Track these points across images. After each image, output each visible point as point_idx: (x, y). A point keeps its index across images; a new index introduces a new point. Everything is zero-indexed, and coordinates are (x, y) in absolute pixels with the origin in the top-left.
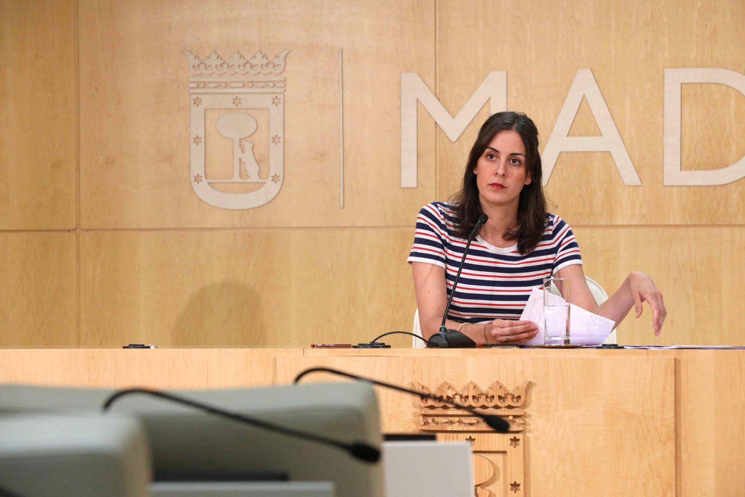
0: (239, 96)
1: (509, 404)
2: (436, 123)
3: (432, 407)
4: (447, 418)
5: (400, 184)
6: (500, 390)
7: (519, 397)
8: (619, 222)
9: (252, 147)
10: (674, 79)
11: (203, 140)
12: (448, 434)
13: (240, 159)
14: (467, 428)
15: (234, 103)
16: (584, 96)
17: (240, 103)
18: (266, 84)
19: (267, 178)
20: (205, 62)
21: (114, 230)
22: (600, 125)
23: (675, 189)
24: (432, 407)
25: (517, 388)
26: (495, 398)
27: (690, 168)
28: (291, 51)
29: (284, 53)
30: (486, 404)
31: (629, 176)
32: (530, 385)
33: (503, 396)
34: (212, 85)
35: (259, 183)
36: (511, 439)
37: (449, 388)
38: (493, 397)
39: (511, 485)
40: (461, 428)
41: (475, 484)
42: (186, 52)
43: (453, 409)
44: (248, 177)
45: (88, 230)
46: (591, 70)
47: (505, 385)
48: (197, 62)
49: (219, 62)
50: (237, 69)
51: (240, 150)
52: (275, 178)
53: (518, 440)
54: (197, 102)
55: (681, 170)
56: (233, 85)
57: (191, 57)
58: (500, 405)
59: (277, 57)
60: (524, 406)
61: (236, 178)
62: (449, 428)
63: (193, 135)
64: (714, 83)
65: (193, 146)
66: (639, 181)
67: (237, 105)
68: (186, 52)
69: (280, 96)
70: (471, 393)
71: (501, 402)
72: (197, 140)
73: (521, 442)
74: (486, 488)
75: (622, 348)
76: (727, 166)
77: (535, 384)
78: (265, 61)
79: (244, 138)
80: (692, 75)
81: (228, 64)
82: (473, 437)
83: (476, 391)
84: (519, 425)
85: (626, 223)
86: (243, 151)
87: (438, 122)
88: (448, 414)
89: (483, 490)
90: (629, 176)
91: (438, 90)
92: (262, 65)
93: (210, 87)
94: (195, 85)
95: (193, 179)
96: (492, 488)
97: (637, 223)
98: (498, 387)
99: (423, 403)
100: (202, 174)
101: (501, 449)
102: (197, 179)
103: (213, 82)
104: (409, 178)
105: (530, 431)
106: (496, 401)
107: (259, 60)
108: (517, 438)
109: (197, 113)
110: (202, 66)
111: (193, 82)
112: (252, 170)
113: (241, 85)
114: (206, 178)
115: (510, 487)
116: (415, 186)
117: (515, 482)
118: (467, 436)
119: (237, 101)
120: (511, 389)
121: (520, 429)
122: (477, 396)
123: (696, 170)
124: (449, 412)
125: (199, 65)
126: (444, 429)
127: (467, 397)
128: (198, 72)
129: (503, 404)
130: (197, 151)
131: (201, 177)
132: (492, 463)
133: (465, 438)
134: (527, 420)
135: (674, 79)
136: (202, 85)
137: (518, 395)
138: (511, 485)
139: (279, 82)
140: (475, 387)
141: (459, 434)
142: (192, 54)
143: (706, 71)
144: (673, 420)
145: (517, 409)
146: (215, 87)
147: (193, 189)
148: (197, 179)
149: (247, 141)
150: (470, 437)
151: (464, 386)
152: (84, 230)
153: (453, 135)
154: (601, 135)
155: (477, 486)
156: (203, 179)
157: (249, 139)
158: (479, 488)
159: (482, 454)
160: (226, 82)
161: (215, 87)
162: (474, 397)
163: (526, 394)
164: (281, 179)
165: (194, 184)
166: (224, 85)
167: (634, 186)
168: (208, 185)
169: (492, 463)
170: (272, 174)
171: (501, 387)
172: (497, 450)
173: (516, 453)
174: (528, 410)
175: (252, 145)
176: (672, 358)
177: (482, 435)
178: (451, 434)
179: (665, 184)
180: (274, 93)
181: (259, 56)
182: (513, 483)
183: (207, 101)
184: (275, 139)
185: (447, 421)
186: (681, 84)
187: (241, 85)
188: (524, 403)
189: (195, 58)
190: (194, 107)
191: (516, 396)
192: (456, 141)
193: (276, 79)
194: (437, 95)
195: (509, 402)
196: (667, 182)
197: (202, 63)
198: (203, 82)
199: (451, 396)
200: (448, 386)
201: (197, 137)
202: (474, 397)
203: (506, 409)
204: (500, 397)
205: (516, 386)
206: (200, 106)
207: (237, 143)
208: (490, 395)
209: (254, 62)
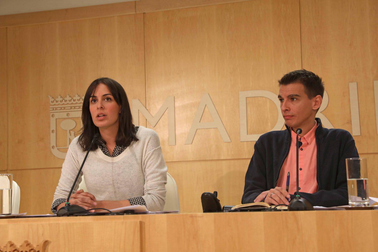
0: (69, 113)
2: (146, 120)
6: (27, 247)
8: (222, 158)
9: (74, 133)
10: (243, 95)
11: (55, 131)
13: (70, 139)
15: (67, 115)
16: (206, 105)
17: (70, 116)
23: (245, 143)
27: (251, 134)
32: (46, 243)
42: (49, 96)
45: (12, 170)
47: (32, 243)
48: (53, 100)
49: (61, 99)
50: (68, 102)
51: (70, 134)
55: (247, 134)
56: (66, 108)
57: (50, 98)
63: (51, 129)
64: (260, 97)
65: (52, 134)
66: (230, 140)
67: (68, 116)
68: (49, 96)
72: (53, 131)
77: (51, 242)
79: (71, 130)
80: (250, 94)
85: (225, 159)
86: (70, 135)
91: (147, 106)
92: (78, 100)
93: (58, 110)
94: (52, 109)
95: (51, 147)
98: (25, 244)
100: (55, 145)
102: (53, 147)
109: (53, 121)
113: (70, 108)
114: (57, 147)
119: (68, 115)
120: (35, 246)
123: (254, 134)
128: (53, 104)
130: (53, 136)
131: (54, 146)
142: (51, 96)
146: (60, 110)
147: (51, 152)
148: (53, 147)
149: (72, 131)
151: (5, 246)
156: (55, 147)
157: (73, 130)
160: (64, 107)
161: (60, 110)
165: (52, 149)
166: (63, 108)
167: (228, 142)
168: (57, 150)
171: (28, 244)
175: (74, 132)
176: (138, 221)
181: (77, 96)
183: (57, 115)
186: (246, 98)
187: (70, 108)
189: (52, 98)
190: (51, 118)
192: (155, 127)
194: (147, 108)
197: (55, 100)
198: (55, 108)
205: (38, 245)
206: (54, 117)
207: (68, 132)
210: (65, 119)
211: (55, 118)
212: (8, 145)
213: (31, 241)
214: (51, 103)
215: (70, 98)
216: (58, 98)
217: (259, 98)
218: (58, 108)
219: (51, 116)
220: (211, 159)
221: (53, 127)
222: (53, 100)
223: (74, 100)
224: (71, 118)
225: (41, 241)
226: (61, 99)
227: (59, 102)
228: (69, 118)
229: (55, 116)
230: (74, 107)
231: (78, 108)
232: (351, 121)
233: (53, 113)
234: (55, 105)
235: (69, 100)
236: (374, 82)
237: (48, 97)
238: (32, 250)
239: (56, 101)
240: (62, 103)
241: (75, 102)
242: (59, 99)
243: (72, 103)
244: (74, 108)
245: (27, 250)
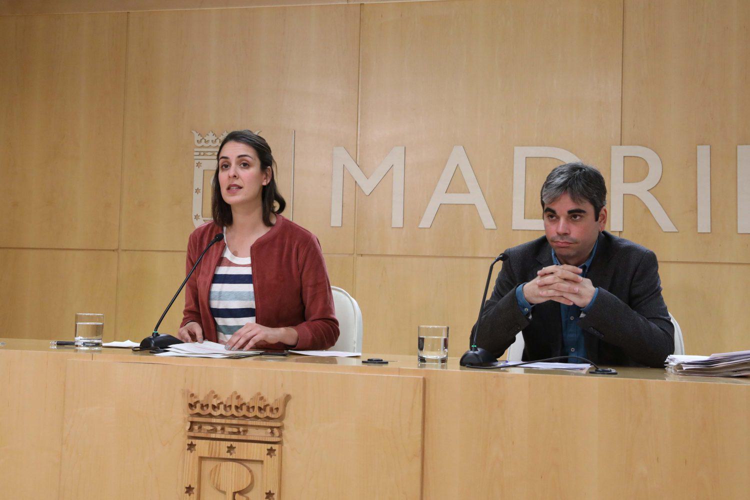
1: (268, 415)
2: (356, 182)
3: (199, 415)
4: (214, 425)
6: (260, 401)
7: (277, 409)
10: (520, 154)
11: (201, 191)
12: (212, 441)
14: (228, 437)
20: (205, 138)
22: (469, 185)
24: (199, 415)
25: (276, 400)
26: (255, 408)
27: (531, 218)
30: (247, 414)
32: (288, 398)
33: (262, 407)
36: (268, 450)
37: (216, 396)
38: (253, 407)
39: (267, 493)
40: (223, 436)
41: (233, 491)
42: (193, 131)
43: (219, 417)
45: (126, 250)
46: (463, 147)
48: (199, 138)
49: (214, 138)
53: (275, 450)
54: (199, 165)
57: (196, 135)
58: (259, 416)
60: (281, 418)
62: (213, 436)
63: (195, 187)
65: (195, 194)
68: (193, 131)
70: (235, 403)
71: (261, 413)
72: (197, 191)
73: (276, 452)
74: (246, 495)
75: (387, 363)
81: (220, 140)
82: (234, 446)
83: (238, 402)
88: (212, 422)
89: (241, 497)
91: (358, 159)
93: (208, 155)
94: (198, 154)
95: (194, 217)
96: (249, 495)
98: (258, 399)
99: (190, 410)
100: (200, 214)
101: (258, 459)
102: (197, 217)
106: (256, 412)
108: (274, 448)
110: (203, 141)
117: (270, 491)
118: (229, 444)
120: (271, 401)
122: (239, 406)
123: (535, 219)
124: (214, 420)
126: (209, 437)
127: (230, 406)
128: (200, 145)
129: (262, 415)
132: (251, 471)
133: (226, 446)
134: (284, 432)
135: (520, 154)
137: (276, 407)
138: (267, 493)
140: (238, 397)
141: (221, 442)
143: (542, 148)
148: (197, 217)
150: (231, 445)
155: (235, 493)
156: (201, 217)
158: (237, 495)
159: (242, 462)
162: (237, 407)
163: (285, 405)
169: (251, 471)
171: (262, 398)
172: (254, 459)
173: (271, 463)
174: (285, 422)
177: (242, 443)
178: (214, 442)
179: (513, 228)
182: (268, 492)
185: (211, 428)
188: (281, 416)
190: (196, 168)
191: (274, 408)
194: (358, 163)
195: (268, 413)
199: (216, 405)
200: (213, 395)
201: (198, 189)
202: (237, 407)
204: (260, 409)
208: (251, 406)
211: (201, 169)
212: (121, 210)
213: (263, 394)
216: (208, 135)
217: (548, 159)
219: (196, 165)
220: (461, 256)
222: (199, 138)
227: (210, 143)
229: (202, 165)
232: (697, 209)
233: (200, 161)
236: (739, 147)
237: (193, 134)
238: (268, 405)
239: (205, 140)
245: (260, 406)
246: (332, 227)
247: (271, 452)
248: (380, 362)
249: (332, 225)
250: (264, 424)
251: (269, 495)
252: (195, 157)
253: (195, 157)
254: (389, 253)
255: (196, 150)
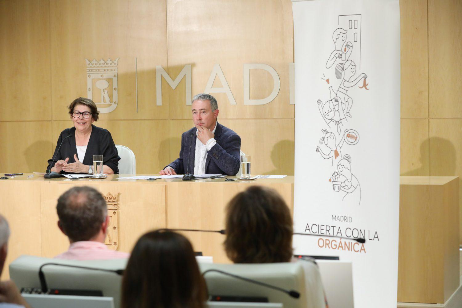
5: (156, 104)
8: (229, 118)
11: (91, 90)
18: (112, 70)
19: (112, 102)
21: (64, 121)
28: (119, 58)
29: (117, 59)
31: (232, 102)
32: (119, 194)
34: (94, 70)
35: (110, 104)
36: (113, 212)
42: (86, 59)
44: (106, 102)
47: (112, 194)
48: (89, 63)
49: (96, 62)
52: (115, 103)
54: (89, 76)
56: (101, 70)
57: (87, 61)
59: (115, 60)
60: (117, 201)
61: (102, 103)
63: (88, 88)
65: (88, 91)
69: (116, 74)
72: (89, 89)
73: (116, 213)
76: (265, 98)
77: (121, 194)
78: (111, 62)
79: (105, 89)
84: (116, 208)
86: (104, 93)
87: (169, 83)
90: (232, 102)
92: (110, 64)
94: (88, 70)
97: (235, 118)
103: (95, 69)
104: (159, 102)
105: (120, 209)
107: (109, 62)
109: (89, 81)
111: (88, 69)
112: (107, 99)
115: (113, 228)
116: (161, 105)
120: (113, 195)
121: (116, 209)
125: (90, 63)
128: (89, 66)
134: (119, 206)
136: (91, 70)
139: (116, 69)
142: (87, 59)
144: (165, 206)
145: (116, 202)
152: (54, 121)
153: (174, 88)
154: (223, 87)
160: (98, 70)
164: (117, 103)
166: (98, 70)
170: (114, 101)
171: (110, 194)
180: (114, 73)
181: (109, 60)
183: (93, 76)
184: (115, 89)
190: (88, 78)
193: (115, 68)
195: (112, 200)
196: (245, 104)
203: (112, 202)
204: (110, 198)
209: (107, 62)
210: (100, 79)
213: (111, 193)
214: (87, 64)
215: (104, 62)
218: (94, 69)
219: (88, 76)
221: (89, 86)
222: (89, 63)
223: (107, 64)
224: (104, 79)
225: (117, 193)
226: (96, 62)
227: (94, 65)
228: (103, 79)
230: (107, 69)
231: (111, 71)
234: (90, 67)
235: (103, 64)
240: (97, 66)
241: (107, 66)
242: (94, 62)
243: (105, 67)
244: (107, 71)
246: (157, 106)
247: (114, 212)
248: (153, 179)
249: (157, 105)
250: (111, 203)
251: (115, 228)
252: (87, 72)
253: (87, 72)
254: (186, 118)
255: (87, 68)
